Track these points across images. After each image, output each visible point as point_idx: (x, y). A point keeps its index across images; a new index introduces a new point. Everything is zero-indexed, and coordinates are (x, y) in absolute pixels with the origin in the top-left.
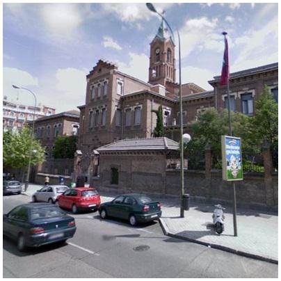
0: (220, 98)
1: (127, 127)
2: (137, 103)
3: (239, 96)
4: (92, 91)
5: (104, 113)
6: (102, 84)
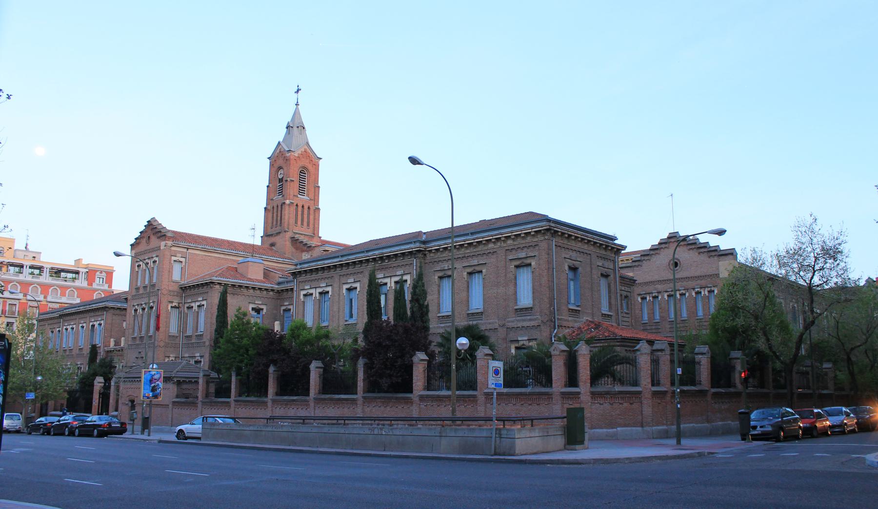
1: (187, 337)
3: (318, 295)
4: (138, 272)
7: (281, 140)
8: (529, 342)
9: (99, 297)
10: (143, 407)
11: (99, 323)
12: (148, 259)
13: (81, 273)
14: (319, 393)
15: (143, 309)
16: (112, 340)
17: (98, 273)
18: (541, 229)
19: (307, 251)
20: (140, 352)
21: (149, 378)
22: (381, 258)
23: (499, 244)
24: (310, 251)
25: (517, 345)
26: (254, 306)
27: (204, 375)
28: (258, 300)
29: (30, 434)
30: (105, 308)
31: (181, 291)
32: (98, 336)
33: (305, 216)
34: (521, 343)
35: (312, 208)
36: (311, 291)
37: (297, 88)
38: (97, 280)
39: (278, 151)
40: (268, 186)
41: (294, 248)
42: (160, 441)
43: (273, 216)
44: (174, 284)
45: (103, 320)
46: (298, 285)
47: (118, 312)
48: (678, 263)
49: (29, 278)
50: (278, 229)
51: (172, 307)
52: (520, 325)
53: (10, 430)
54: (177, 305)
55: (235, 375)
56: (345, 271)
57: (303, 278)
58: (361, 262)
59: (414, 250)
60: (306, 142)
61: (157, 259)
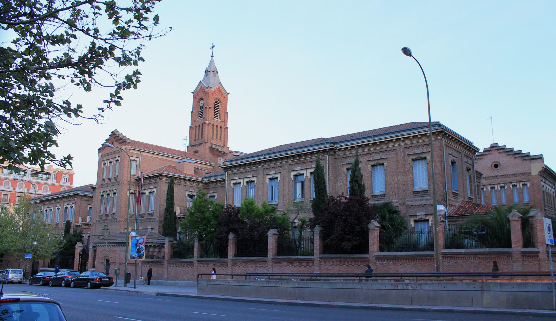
0: (229, 184)
1: (141, 214)
3: (245, 184)
4: (104, 168)
5: (115, 198)
6: (114, 161)
7: (202, 80)
8: (426, 217)
9: (64, 190)
10: (125, 265)
11: (71, 206)
12: (112, 158)
13: (52, 175)
14: (275, 255)
15: (108, 195)
16: (80, 218)
17: (63, 175)
18: (435, 131)
19: (222, 157)
20: (106, 226)
21: (135, 242)
22: (299, 156)
23: (398, 143)
24: (224, 156)
25: (415, 219)
26: (189, 193)
27: (169, 241)
28: (192, 189)
29: (31, 284)
30: (76, 196)
32: (70, 215)
33: (219, 133)
34: (419, 217)
35: (223, 127)
36: (239, 181)
37: (212, 45)
38: (63, 180)
39: (200, 88)
40: (192, 112)
41: (212, 154)
42: (158, 294)
43: (196, 132)
46: (228, 177)
47: (84, 198)
48: (499, 164)
50: (200, 141)
52: (418, 203)
53: (14, 281)
54: (133, 191)
55: (197, 240)
56: (268, 165)
57: (233, 171)
58: (282, 158)
59: (327, 148)
60: (219, 82)
61: (119, 159)
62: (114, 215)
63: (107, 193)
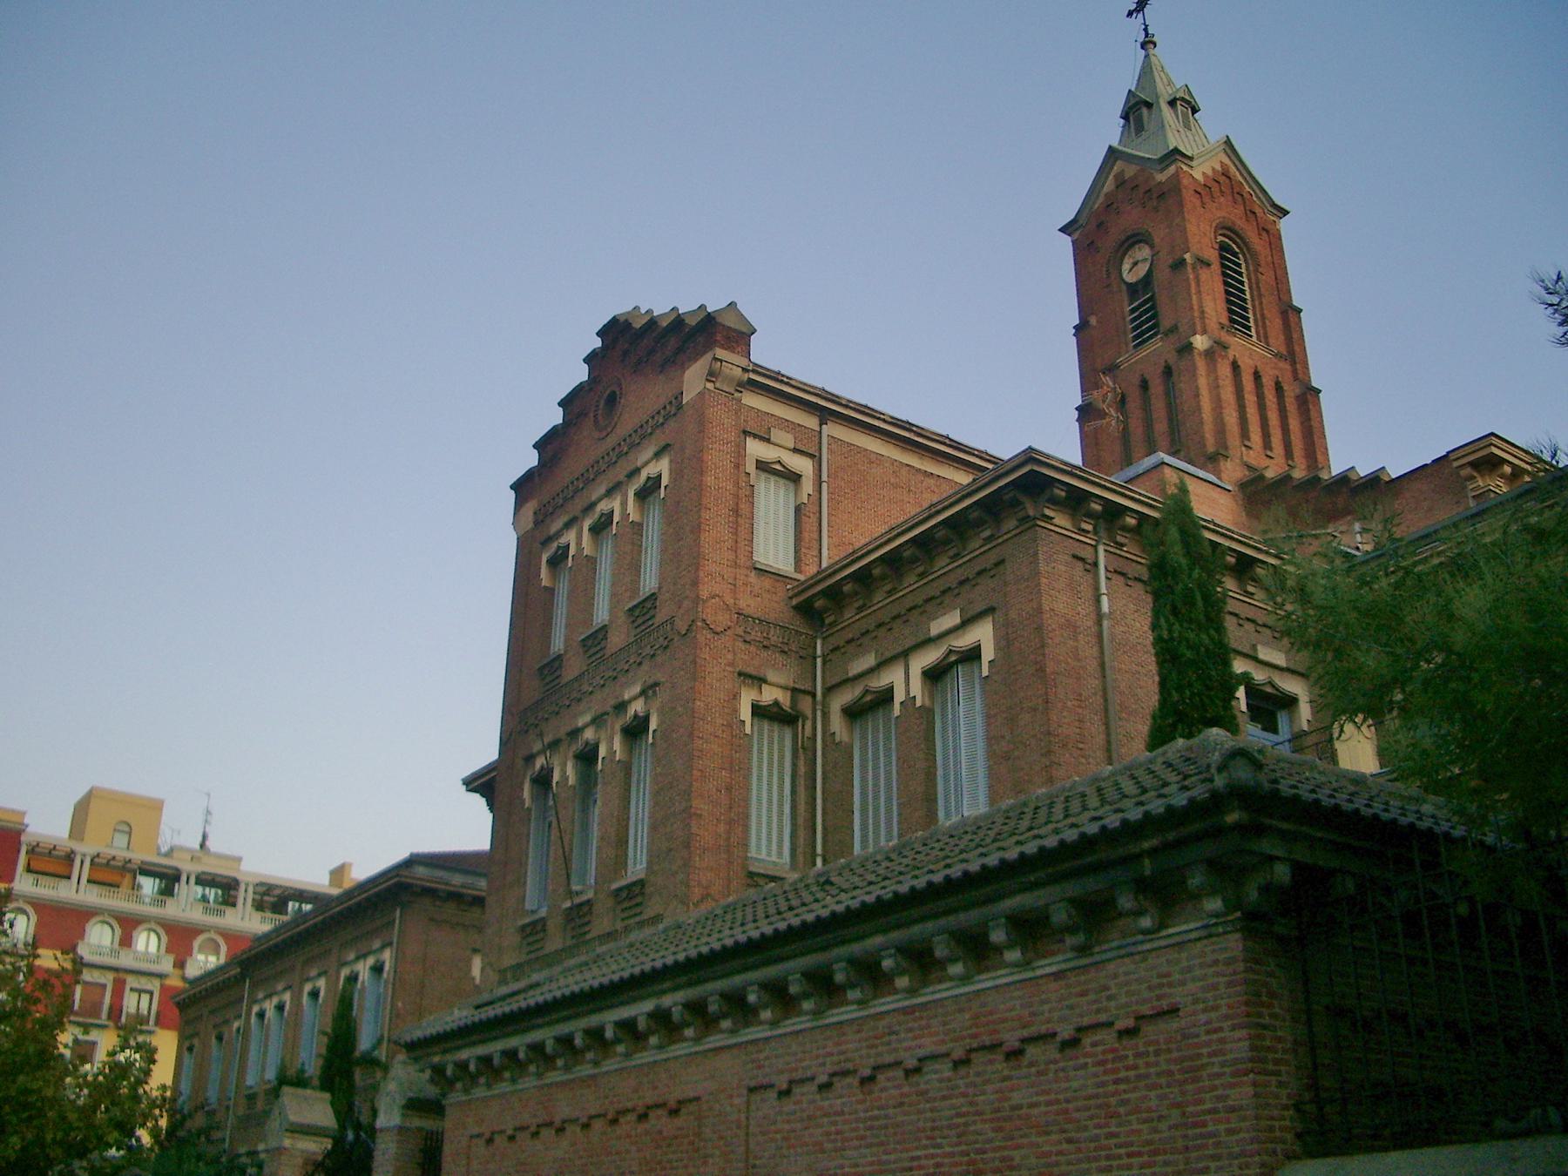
2: (952, 619)
4: (551, 591)
5: (644, 768)
6: (623, 506)
31: (798, 624)
35: (1291, 391)
39: (1109, 185)
44: (767, 583)
45: (390, 944)
49: (196, 915)
51: (758, 711)
54: (784, 698)
61: (663, 467)
62: (633, 895)
63: (578, 746)
